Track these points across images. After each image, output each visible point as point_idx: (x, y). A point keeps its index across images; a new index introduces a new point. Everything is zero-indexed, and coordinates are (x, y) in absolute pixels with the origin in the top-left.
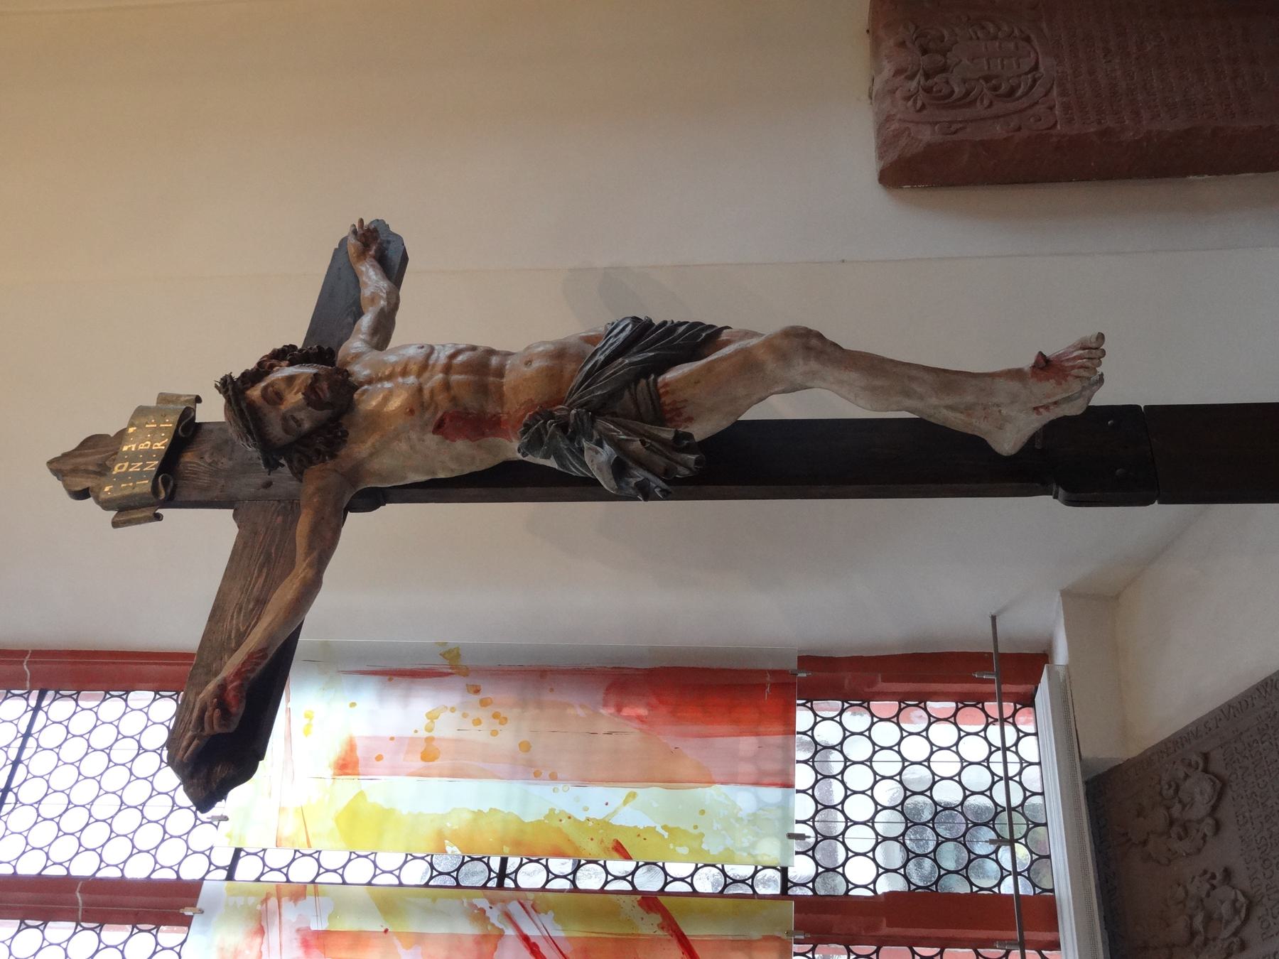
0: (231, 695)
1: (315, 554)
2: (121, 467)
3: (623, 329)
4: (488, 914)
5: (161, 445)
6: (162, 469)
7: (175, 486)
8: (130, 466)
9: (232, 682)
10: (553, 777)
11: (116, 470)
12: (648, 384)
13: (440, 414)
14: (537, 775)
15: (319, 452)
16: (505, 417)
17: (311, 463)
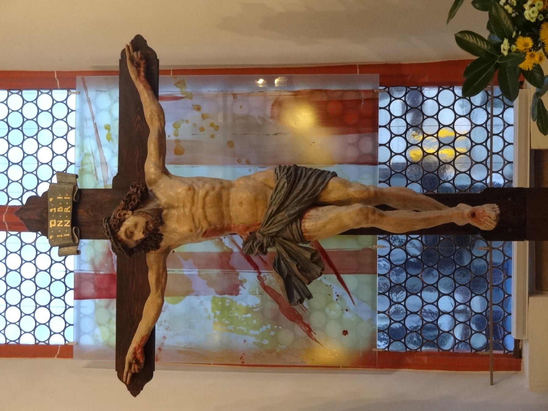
0: (139, 356)
1: (160, 291)
2: (53, 223)
3: (283, 185)
4: (223, 241)
5: (68, 210)
6: (73, 224)
7: (80, 231)
8: (57, 223)
9: (138, 349)
10: (248, 163)
11: (51, 226)
12: (297, 226)
13: (204, 230)
14: (239, 161)
15: (152, 246)
16: (233, 226)
17: (149, 252)
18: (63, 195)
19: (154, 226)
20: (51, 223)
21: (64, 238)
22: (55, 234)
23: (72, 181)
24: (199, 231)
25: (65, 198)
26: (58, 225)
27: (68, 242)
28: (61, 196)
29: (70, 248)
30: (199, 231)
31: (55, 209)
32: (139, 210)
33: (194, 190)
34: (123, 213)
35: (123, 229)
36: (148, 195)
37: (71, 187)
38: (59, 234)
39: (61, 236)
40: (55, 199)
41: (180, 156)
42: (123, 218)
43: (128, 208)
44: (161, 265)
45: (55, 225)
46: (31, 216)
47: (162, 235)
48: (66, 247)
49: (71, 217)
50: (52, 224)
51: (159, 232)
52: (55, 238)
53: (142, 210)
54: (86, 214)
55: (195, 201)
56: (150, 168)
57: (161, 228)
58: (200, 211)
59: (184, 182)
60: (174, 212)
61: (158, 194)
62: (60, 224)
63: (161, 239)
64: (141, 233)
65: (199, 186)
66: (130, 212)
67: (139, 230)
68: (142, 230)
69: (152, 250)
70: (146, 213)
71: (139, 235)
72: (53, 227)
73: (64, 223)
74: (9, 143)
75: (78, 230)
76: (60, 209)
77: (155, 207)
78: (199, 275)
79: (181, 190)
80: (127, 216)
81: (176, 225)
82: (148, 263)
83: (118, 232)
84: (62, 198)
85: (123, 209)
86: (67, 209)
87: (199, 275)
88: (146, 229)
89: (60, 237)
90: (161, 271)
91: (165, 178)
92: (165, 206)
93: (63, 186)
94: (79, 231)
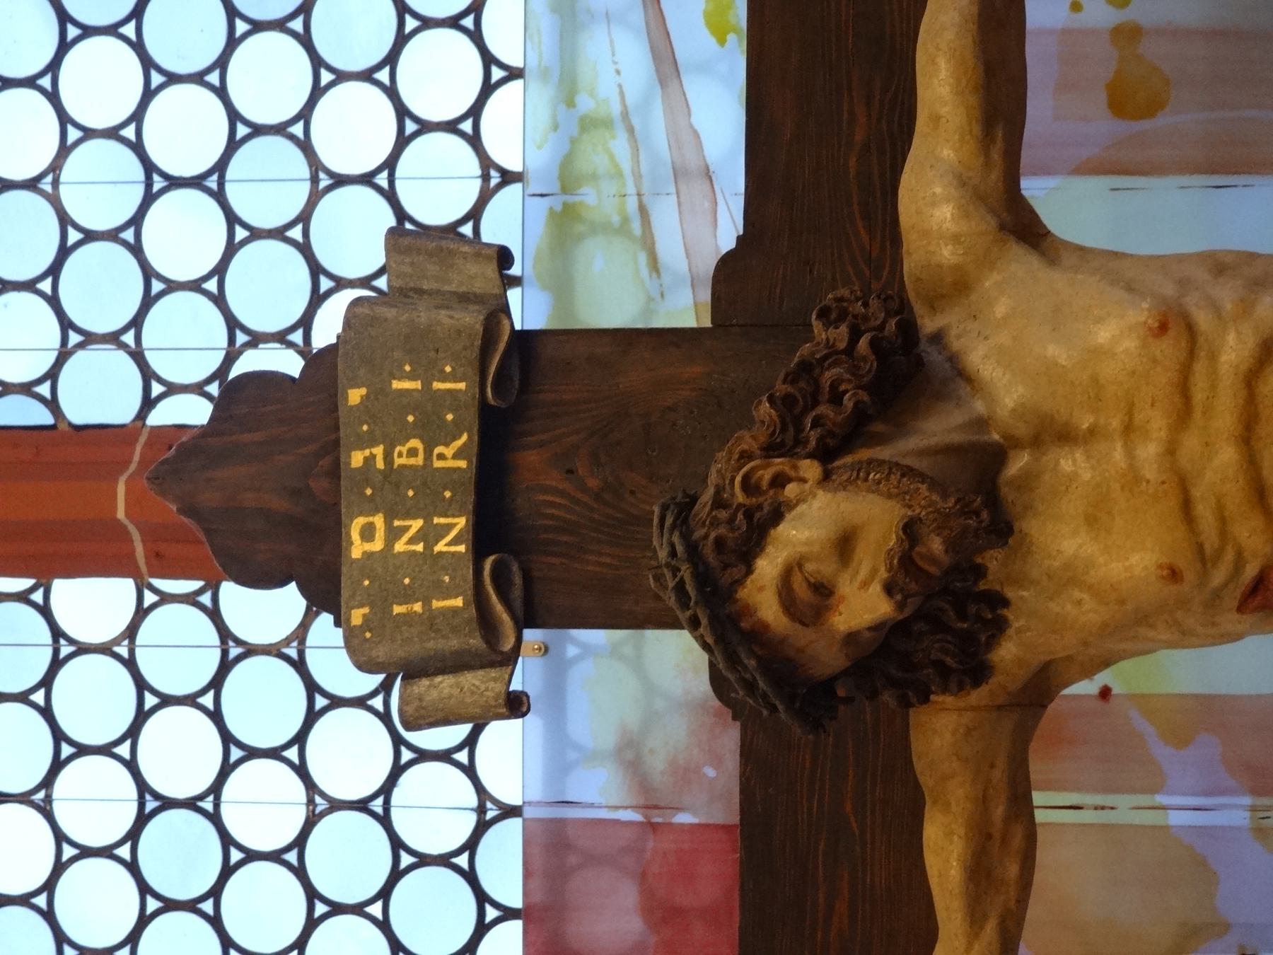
1: (990, 929)
2: (368, 533)
5: (453, 456)
8: (393, 534)
11: (357, 549)
13: (1251, 571)
15: (940, 666)
17: (925, 700)
18: (428, 372)
19: (950, 546)
20: (355, 535)
21: (431, 621)
22: (380, 601)
23: (478, 287)
24: (1218, 577)
25: (437, 385)
26: (400, 547)
27: (454, 643)
28: (411, 377)
29: (471, 679)
30: (1218, 577)
31: (379, 451)
32: (865, 454)
33: (1191, 330)
34: (767, 475)
35: (768, 567)
36: (919, 363)
37: (472, 319)
38: (407, 598)
39: (418, 607)
40: (379, 393)
41: (1145, 125)
42: (766, 501)
43: (799, 441)
44: (999, 775)
45: (377, 545)
46: (241, 490)
47: (1006, 603)
48: (443, 671)
49: (471, 499)
50: (364, 538)
51: (982, 586)
52: (380, 622)
53: (884, 453)
54: (554, 479)
55: (1199, 396)
56: (933, 203)
57: (993, 560)
58: (1227, 455)
59: (1130, 288)
60: (1070, 462)
61: (980, 357)
62: (407, 540)
63: (999, 627)
64: (876, 588)
65: (1217, 310)
66: (811, 469)
67: (864, 572)
68: (883, 574)
69: (945, 690)
70: (908, 472)
71: (863, 604)
72: (368, 555)
73: (429, 535)
74: (148, 64)
75: (515, 568)
76: (410, 453)
77: (957, 438)
78: (1260, 832)
79: (1116, 333)
80: (791, 490)
81: (1089, 542)
82: (919, 766)
83: (740, 582)
84: (417, 385)
85: (771, 450)
86: (449, 452)
87: (1260, 832)
88: (906, 569)
89: (408, 618)
90: (999, 812)
91: (1021, 261)
92: (1022, 430)
93: (424, 314)
94: (518, 580)
